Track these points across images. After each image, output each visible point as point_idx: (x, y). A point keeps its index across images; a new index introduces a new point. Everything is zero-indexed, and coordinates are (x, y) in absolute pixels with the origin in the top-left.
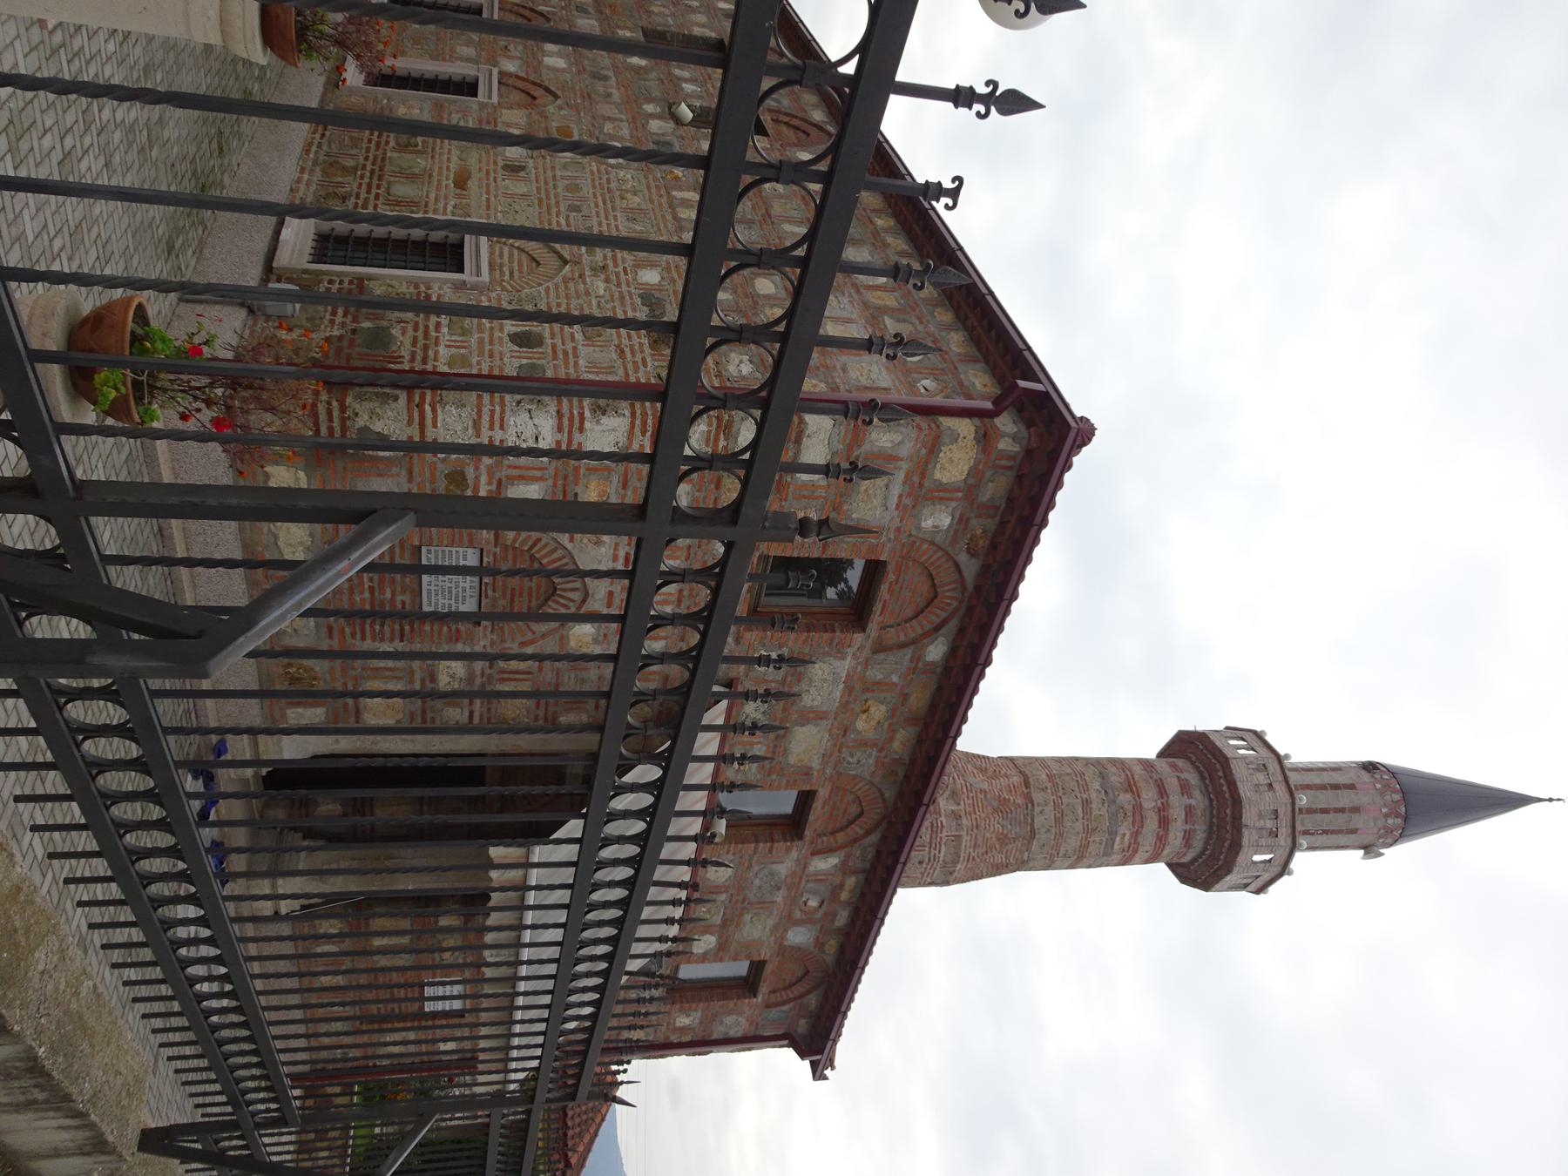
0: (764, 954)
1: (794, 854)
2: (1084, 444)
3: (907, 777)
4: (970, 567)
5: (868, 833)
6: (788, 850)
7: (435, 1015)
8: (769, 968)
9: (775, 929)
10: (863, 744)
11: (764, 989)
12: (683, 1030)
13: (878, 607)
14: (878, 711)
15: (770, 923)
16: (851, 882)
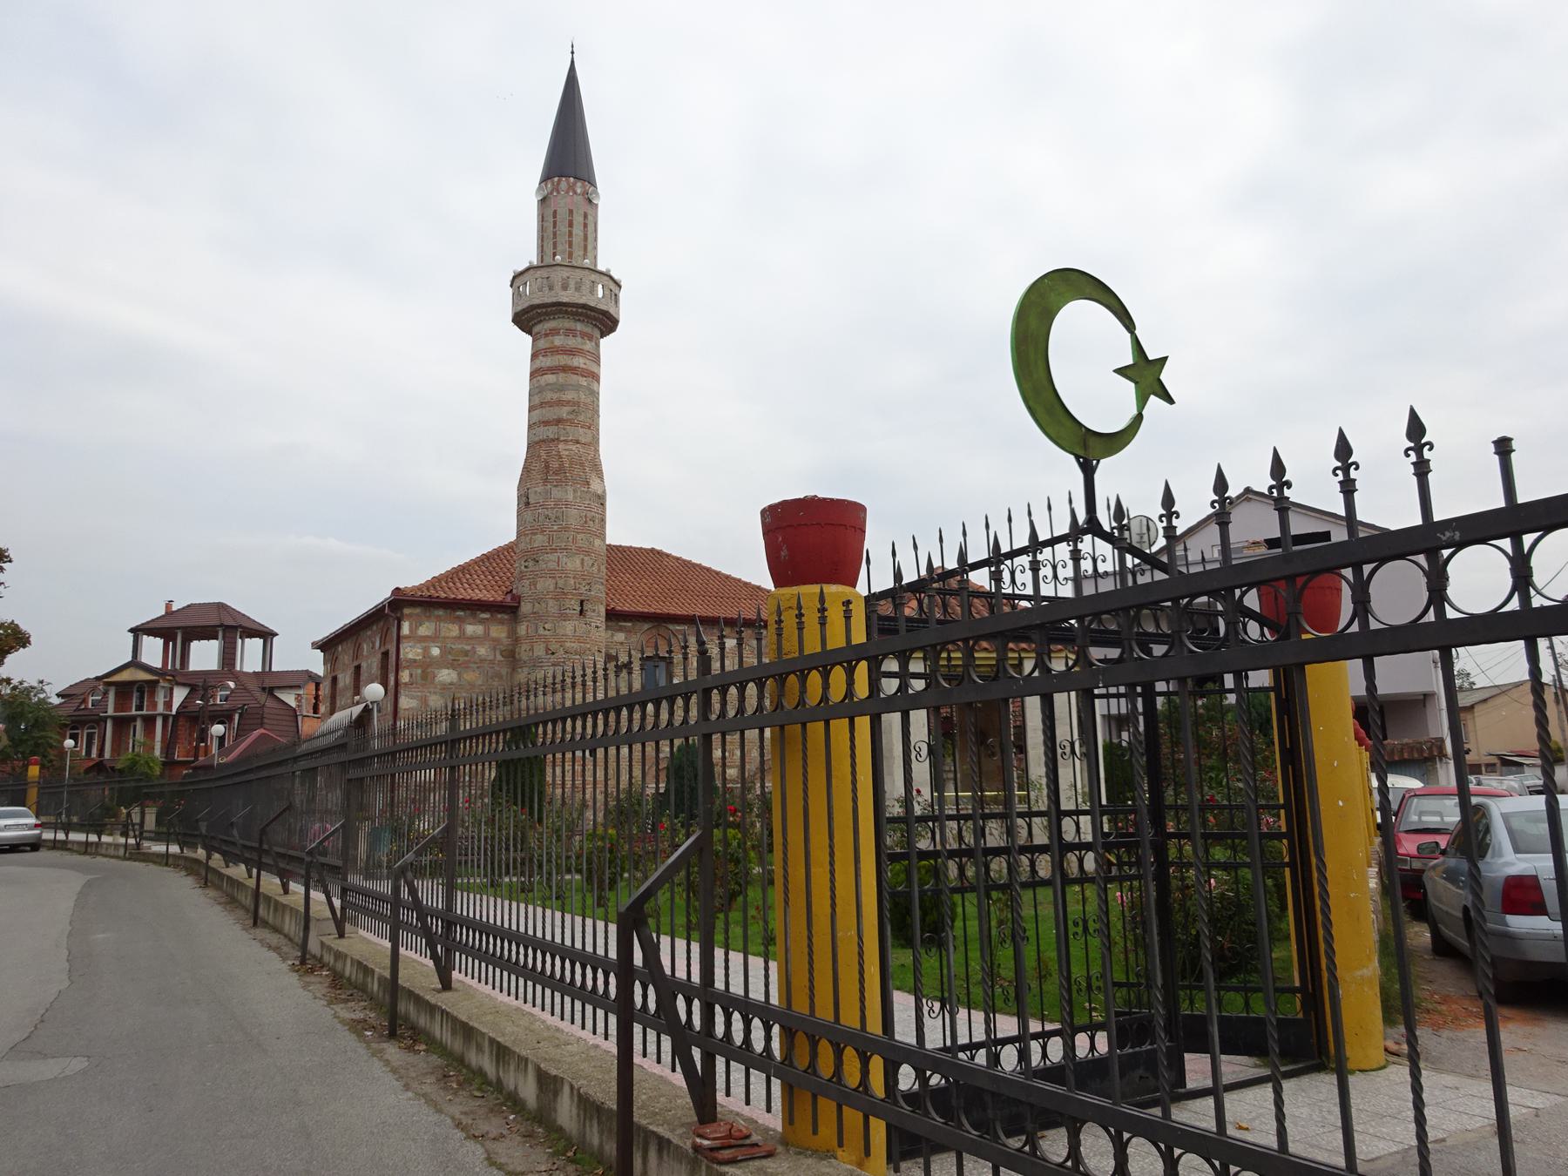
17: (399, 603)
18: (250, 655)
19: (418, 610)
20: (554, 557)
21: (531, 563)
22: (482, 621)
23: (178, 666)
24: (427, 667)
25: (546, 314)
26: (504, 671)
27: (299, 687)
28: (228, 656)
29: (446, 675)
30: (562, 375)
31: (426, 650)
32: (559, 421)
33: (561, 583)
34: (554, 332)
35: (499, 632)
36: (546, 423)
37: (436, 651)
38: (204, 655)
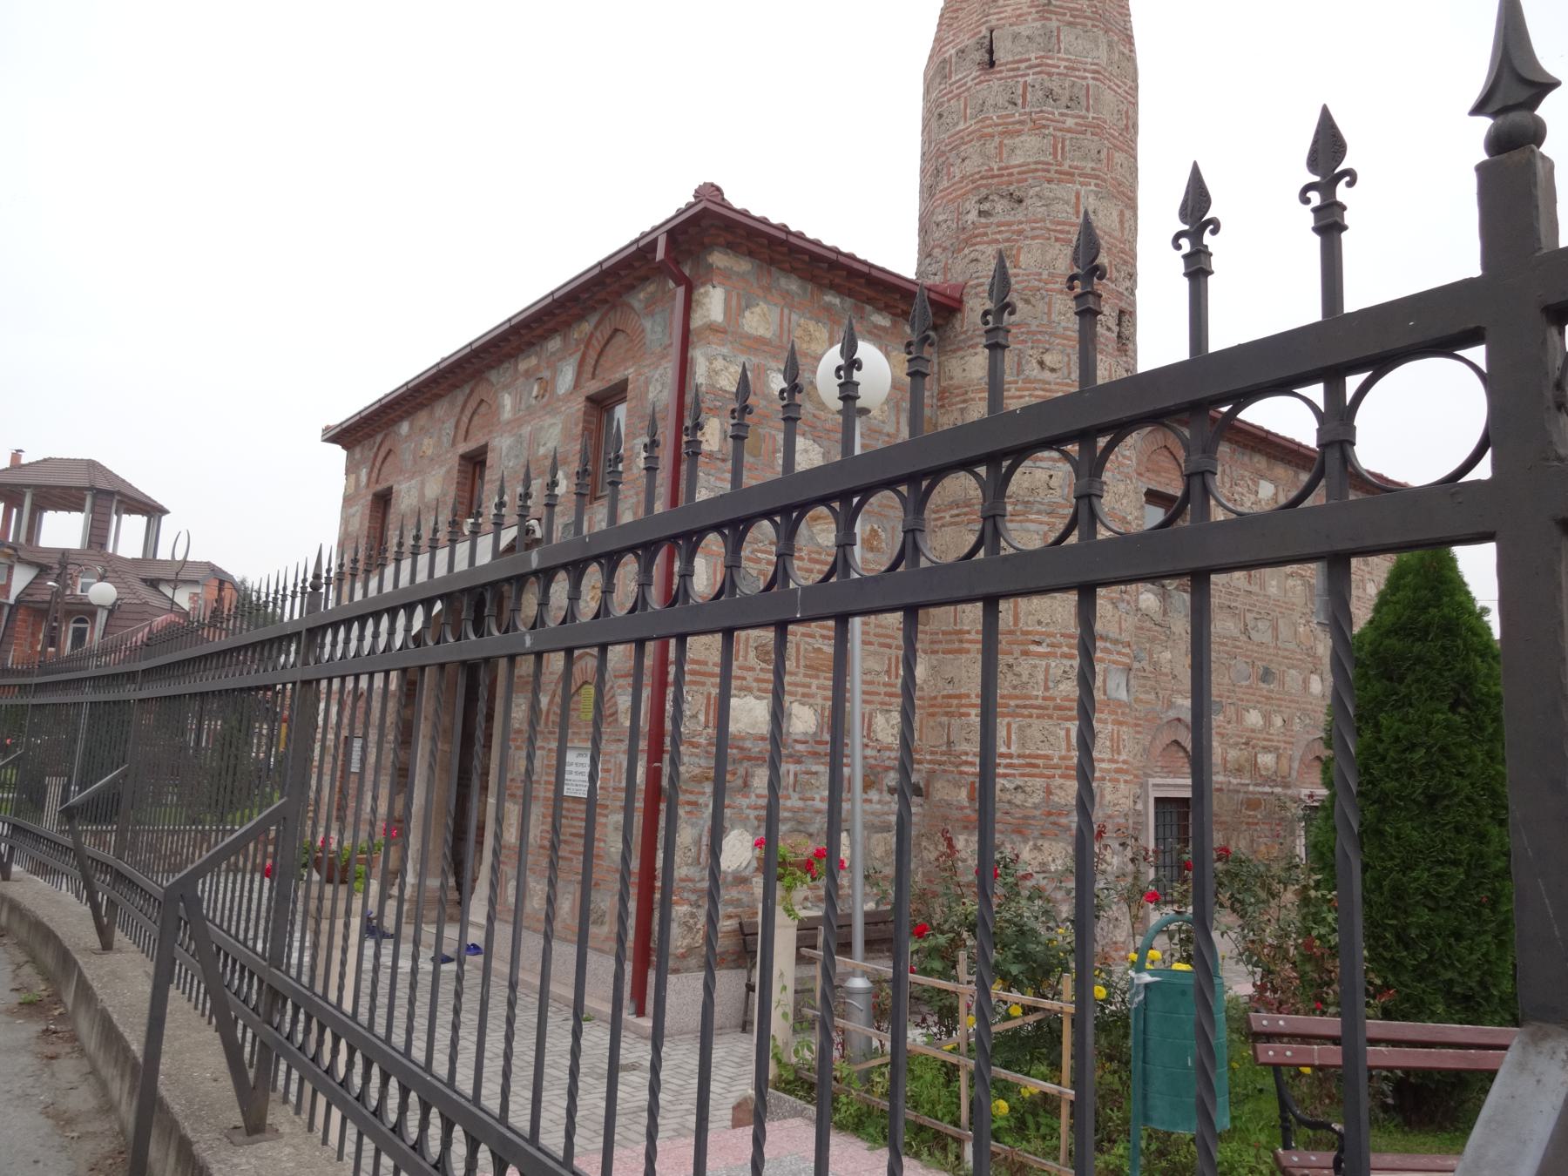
0: (578, 405)
2: (327, 429)
4: (379, 438)
8: (593, 387)
11: (617, 377)
15: (549, 420)
16: (522, 366)
17: (708, 235)
18: (128, 537)
19: (743, 265)
20: (1066, 191)
21: (1000, 206)
23: (22, 539)
27: (195, 582)
28: (97, 535)
38: (62, 530)
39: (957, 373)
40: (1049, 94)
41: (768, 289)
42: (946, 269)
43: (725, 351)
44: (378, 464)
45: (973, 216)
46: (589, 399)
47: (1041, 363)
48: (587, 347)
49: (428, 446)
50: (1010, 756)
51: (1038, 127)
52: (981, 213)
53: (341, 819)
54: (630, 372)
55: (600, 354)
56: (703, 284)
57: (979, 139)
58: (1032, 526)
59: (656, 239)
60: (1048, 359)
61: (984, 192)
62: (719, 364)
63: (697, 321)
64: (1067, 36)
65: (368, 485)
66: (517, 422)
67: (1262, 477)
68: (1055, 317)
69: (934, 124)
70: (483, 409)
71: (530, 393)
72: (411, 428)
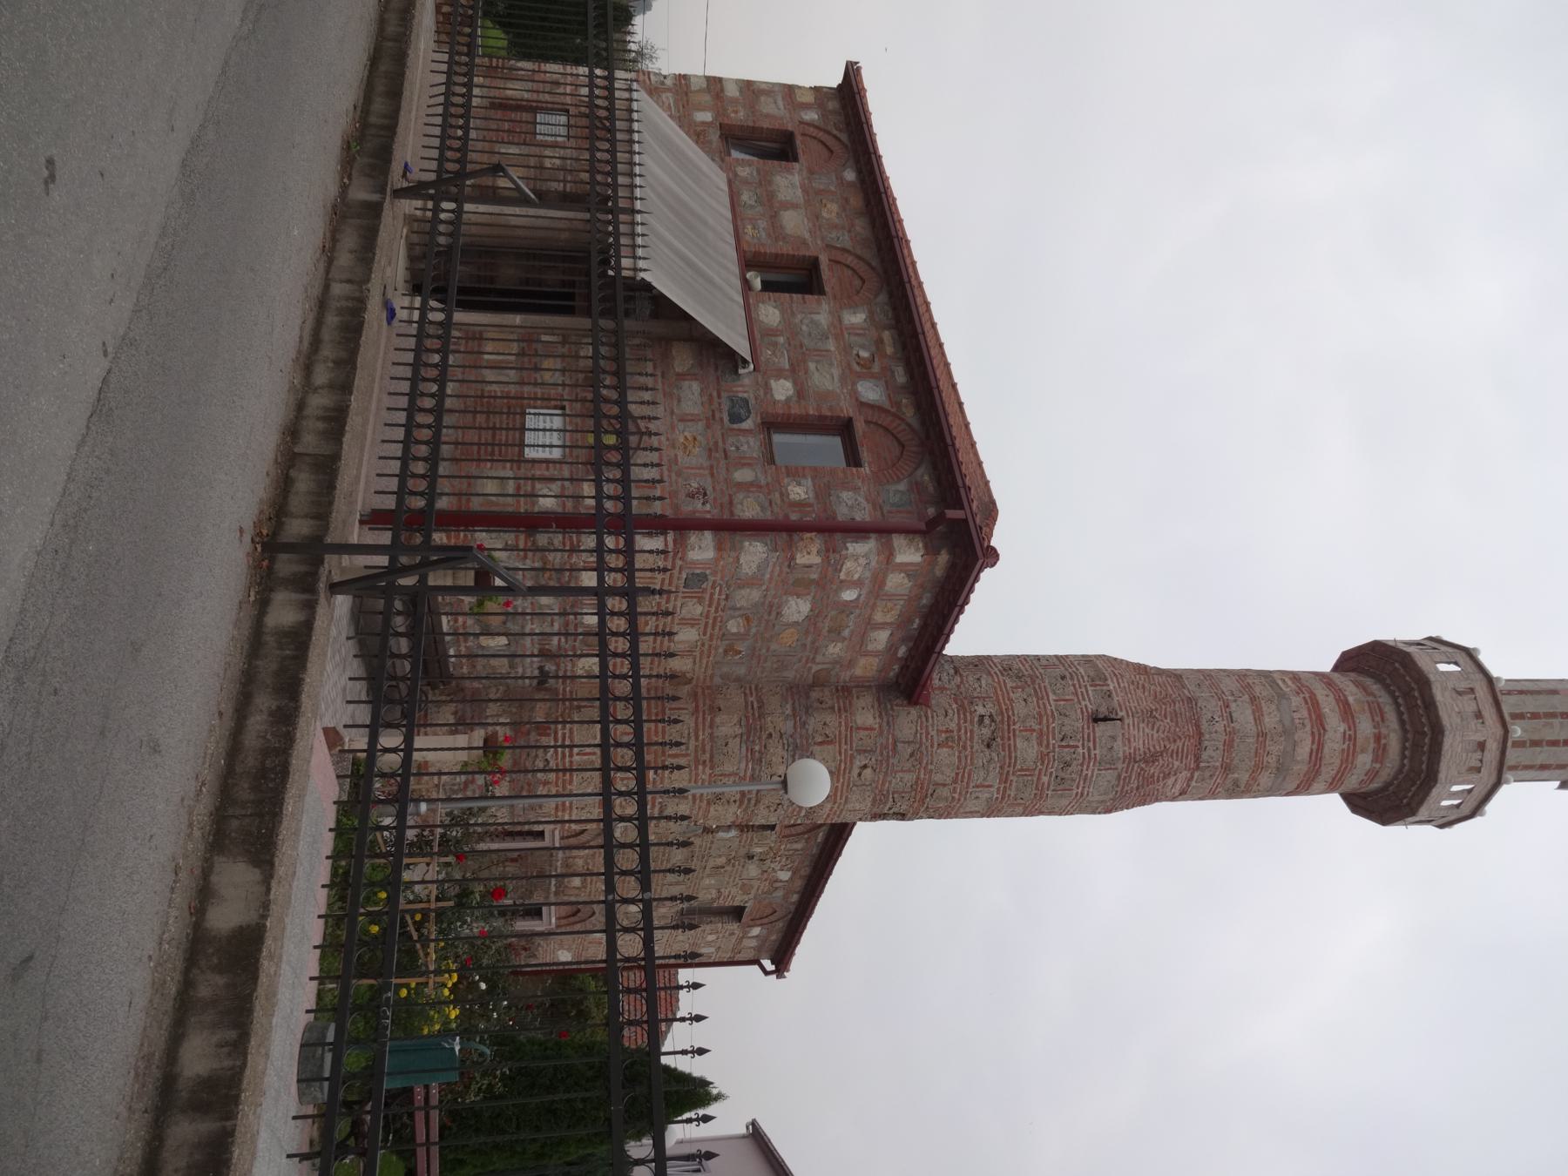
0: (846, 409)
1: (825, 306)
2: (859, 69)
3: (879, 250)
4: (844, 137)
5: (876, 296)
6: (819, 303)
7: (534, 461)
8: (860, 427)
9: (843, 379)
10: (836, 226)
11: (865, 455)
12: (800, 504)
13: (800, 151)
14: (834, 207)
15: (836, 372)
16: (886, 335)
19: (939, 572)
20: (994, 779)
21: (986, 732)
22: (892, 647)
24: (823, 585)
25: (1416, 746)
26: (790, 675)
29: (798, 609)
30: (1305, 768)
31: (858, 584)
32: (1227, 768)
33: (945, 792)
34: (1380, 753)
35: (866, 667)
36: (1229, 745)
37: (849, 595)
39: (861, 703)
40: (1067, 764)
41: (922, 586)
42: (942, 689)
43: (873, 564)
44: (821, 135)
45: (981, 710)
46: (850, 419)
47: (865, 767)
48: (894, 415)
49: (831, 211)
50: (571, 756)
51: (1043, 757)
52: (982, 717)
53: (493, 106)
54: (866, 470)
55: (886, 429)
56: (926, 547)
57: (1040, 714)
58: (743, 766)
59: (962, 508)
60: (868, 771)
61: (998, 719)
62: (863, 561)
63: (898, 541)
64: (1110, 775)
65: (801, 122)
66: (838, 330)
67: (794, 873)
68: (899, 775)
69: (1061, 670)
70: (857, 282)
71: (863, 347)
72: (850, 184)
